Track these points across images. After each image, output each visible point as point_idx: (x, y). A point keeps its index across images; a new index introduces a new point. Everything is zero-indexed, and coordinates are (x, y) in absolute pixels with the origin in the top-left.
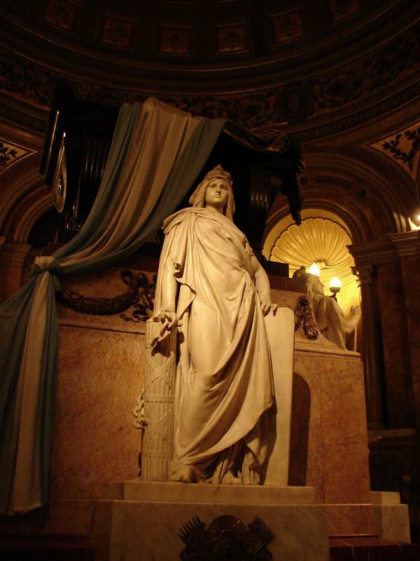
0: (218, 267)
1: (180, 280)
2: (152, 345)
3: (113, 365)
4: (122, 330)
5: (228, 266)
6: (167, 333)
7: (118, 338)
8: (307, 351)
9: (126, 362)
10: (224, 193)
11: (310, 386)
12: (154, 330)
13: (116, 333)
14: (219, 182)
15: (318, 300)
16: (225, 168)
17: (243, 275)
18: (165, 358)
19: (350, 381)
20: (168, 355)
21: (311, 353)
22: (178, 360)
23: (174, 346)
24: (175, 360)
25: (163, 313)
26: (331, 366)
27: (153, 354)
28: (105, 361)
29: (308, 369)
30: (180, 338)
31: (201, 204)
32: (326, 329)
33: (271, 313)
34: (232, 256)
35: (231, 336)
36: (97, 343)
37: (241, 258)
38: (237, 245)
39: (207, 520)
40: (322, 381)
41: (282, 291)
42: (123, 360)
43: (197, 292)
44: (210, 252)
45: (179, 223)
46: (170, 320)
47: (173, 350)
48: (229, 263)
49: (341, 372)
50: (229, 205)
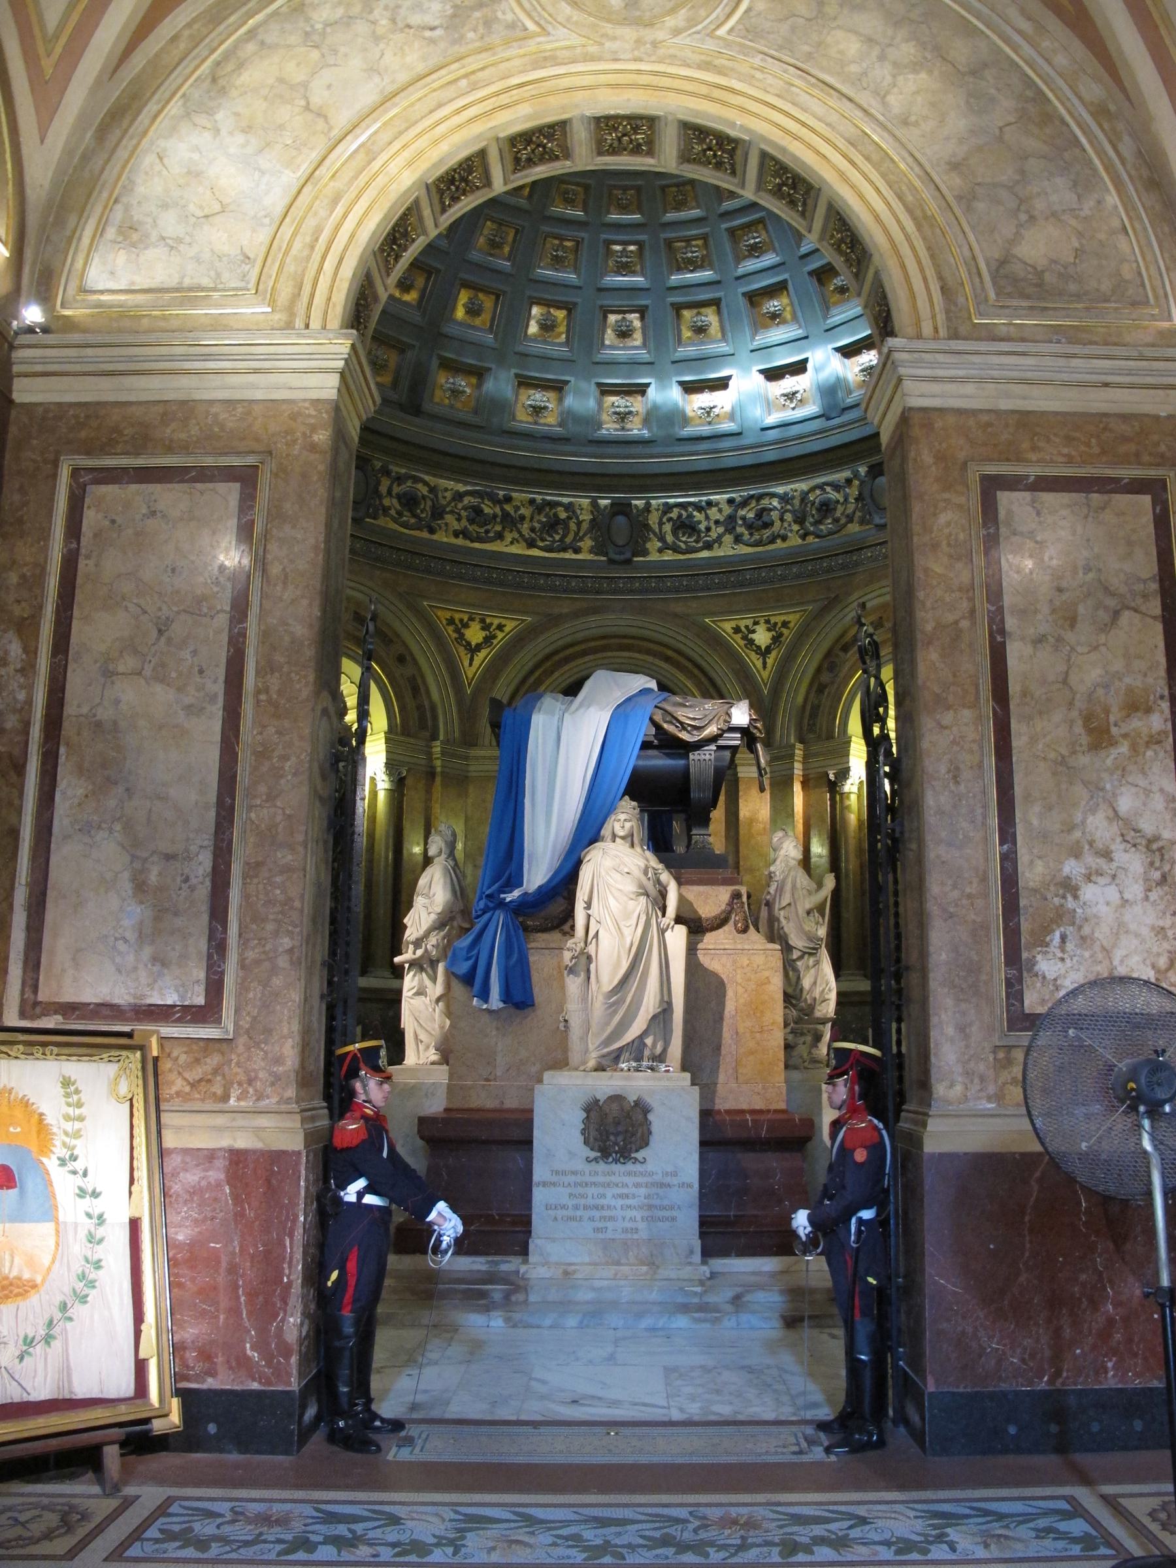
10: (628, 825)
14: (622, 817)
16: (632, 799)
19: (766, 974)
30: (589, 958)
34: (631, 887)
37: (641, 886)
39: (602, 1097)
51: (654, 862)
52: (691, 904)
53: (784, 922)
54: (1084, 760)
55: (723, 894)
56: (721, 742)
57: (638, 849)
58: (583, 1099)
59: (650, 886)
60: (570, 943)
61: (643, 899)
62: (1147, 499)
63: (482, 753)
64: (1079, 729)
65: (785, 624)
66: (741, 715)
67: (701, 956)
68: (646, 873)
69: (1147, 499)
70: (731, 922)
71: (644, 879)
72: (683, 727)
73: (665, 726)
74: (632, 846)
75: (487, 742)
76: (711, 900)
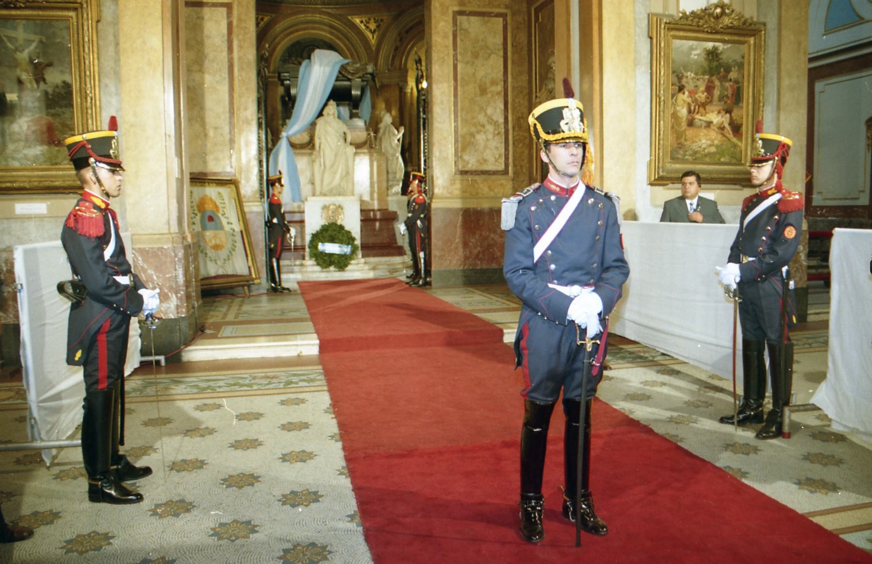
54: (478, 98)
58: (321, 205)
62: (501, 19)
64: (477, 89)
65: (382, 20)
69: (501, 19)
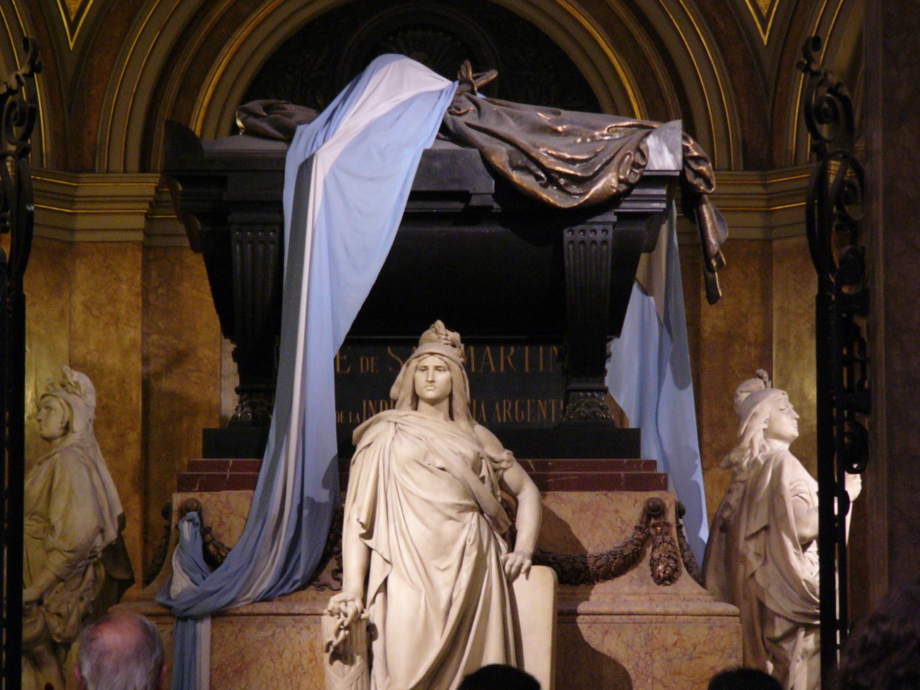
0: (422, 520)
1: (369, 542)
2: (327, 651)
3: (294, 668)
4: (308, 612)
5: (438, 517)
6: (342, 633)
7: (302, 625)
8: (631, 614)
9: (314, 663)
10: (442, 377)
11: (633, 677)
12: (329, 629)
13: (298, 618)
14: (431, 362)
15: (762, 462)
16: (449, 326)
17: (464, 526)
18: (347, 667)
20: (352, 662)
21: (638, 617)
22: (370, 667)
23: (364, 648)
24: (365, 666)
25: (336, 606)
26: (675, 638)
27: (331, 662)
28: (281, 663)
29: (629, 646)
31: (408, 400)
32: (766, 528)
33: (522, 576)
34: (449, 497)
35: (441, 625)
36: (267, 638)
37: (469, 493)
38: (458, 475)
40: (656, 665)
41: (610, 494)
42: (310, 661)
43: (394, 562)
44: (408, 495)
45: (369, 445)
46: (346, 615)
47: (358, 654)
48: (439, 511)
49: (695, 647)
50: (456, 395)
51: (493, 448)
52: (565, 526)
53: (755, 564)
55: (628, 508)
56: (627, 206)
57: (462, 423)
59: (484, 491)
60: (334, 601)
61: (471, 518)
63: (107, 188)
66: (664, 154)
67: (583, 624)
68: (476, 468)
70: (645, 564)
71: (472, 479)
72: (552, 178)
73: (516, 176)
74: (451, 415)
75: (117, 162)
76: (603, 520)
